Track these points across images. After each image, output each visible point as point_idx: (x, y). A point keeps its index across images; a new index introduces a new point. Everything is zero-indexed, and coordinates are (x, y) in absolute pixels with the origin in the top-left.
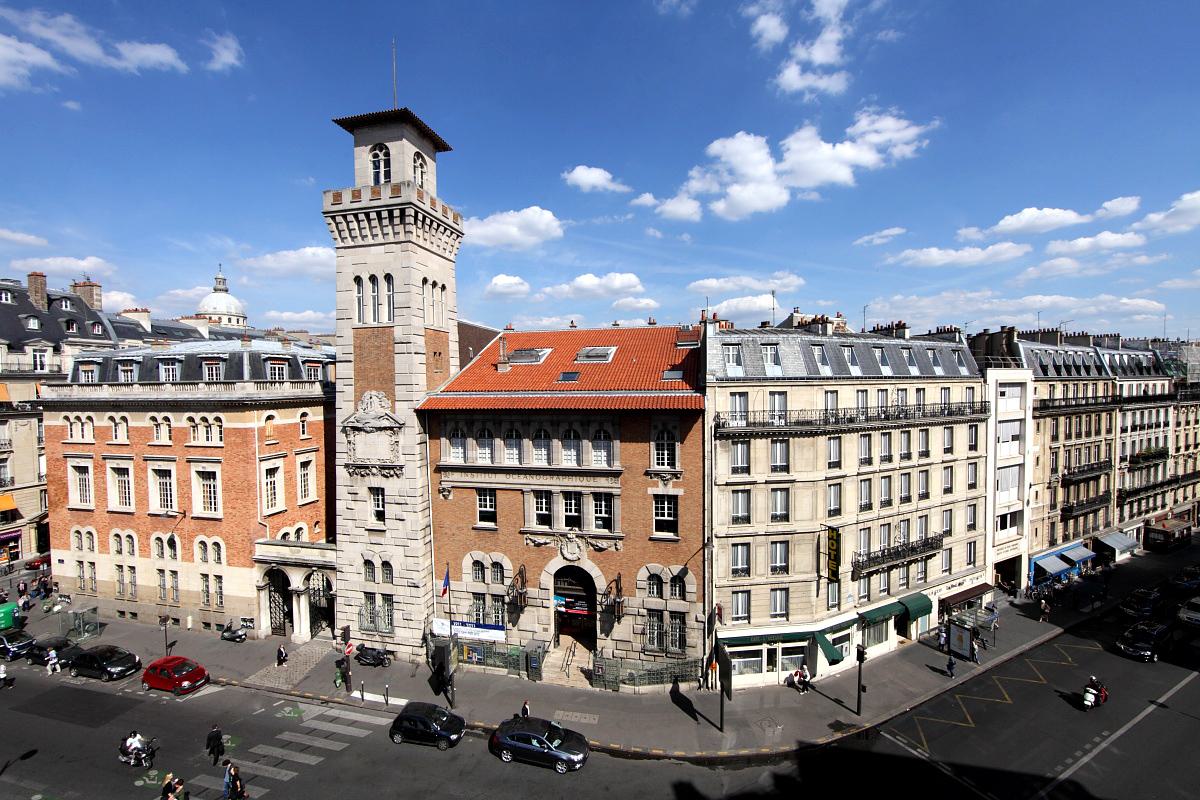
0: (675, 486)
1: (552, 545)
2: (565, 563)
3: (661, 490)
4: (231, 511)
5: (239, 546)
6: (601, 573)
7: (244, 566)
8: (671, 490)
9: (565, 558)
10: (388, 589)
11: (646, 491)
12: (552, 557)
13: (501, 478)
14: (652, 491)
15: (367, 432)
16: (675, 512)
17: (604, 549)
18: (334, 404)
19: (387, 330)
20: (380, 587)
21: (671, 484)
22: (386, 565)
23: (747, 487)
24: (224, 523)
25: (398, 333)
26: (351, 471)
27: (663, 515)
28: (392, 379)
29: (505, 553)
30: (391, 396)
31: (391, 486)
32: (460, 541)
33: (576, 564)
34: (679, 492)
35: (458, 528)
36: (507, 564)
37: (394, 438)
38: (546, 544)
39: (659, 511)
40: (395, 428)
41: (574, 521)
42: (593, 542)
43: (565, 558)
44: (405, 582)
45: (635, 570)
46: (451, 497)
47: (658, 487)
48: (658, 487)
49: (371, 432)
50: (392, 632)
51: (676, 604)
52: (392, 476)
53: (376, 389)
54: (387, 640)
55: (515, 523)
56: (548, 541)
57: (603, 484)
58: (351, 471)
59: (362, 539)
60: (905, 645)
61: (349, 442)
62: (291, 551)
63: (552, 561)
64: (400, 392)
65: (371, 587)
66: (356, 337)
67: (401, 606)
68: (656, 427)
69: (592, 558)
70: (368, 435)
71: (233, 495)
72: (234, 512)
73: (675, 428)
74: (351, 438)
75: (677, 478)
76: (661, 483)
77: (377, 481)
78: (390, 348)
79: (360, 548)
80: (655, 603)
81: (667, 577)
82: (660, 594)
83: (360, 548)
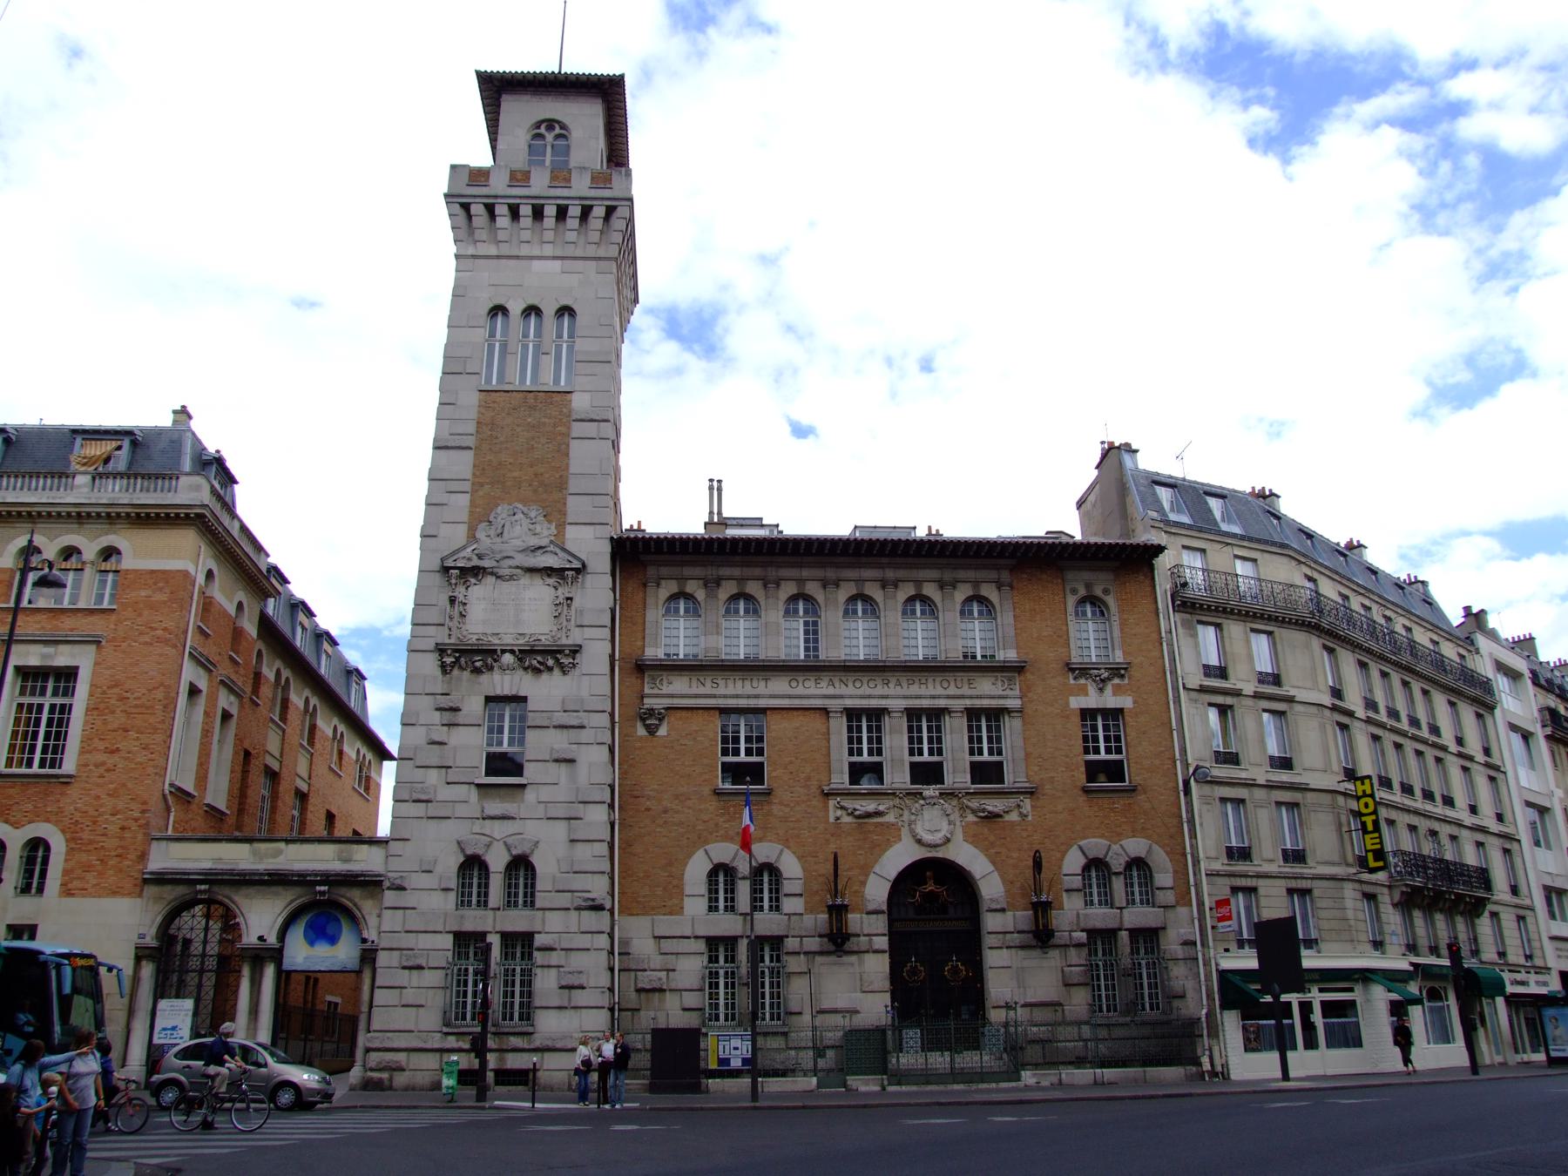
0: (1117, 691)
1: (890, 818)
2: (919, 853)
3: (1092, 700)
4: (101, 757)
5: (111, 843)
6: (992, 868)
7: (114, 893)
8: (1110, 700)
9: (919, 842)
10: (517, 920)
11: (1067, 704)
12: (888, 844)
13: (779, 685)
14: (1076, 703)
15: (498, 577)
16: (1114, 743)
17: (999, 816)
18: (518, 213)
19: (557, 398)
20: (493, 921)
21: (1109, 689)
22: (521, 865)
23: (1229, 700)
24: (73, 791)
25: (580, 402)
26: (449, 660)
27: (1097, 751)
28: (562, 485)
29: (786, 843)
30: (556, 514)
31: (545, 691)
32: (681, 823)
33: (940, 854)
34: (1126, 702)
35: (677, 797)
36: (791, 866)
37: (563, 592)
38: (878, 814)
39: (1089, 743)
40: (566, 574)
41: (927, 774)
42: (974, 804)
43: (919, 842)
44: (564, 900)
45: (1058, 855)
46: (662, 731)
47: (1087, 695)
48: (1087, 695)
49: (511, 578)
50: (527, 1016)
51: (1140, 916)
52: (550, 669)
53: (524, 502)
54: (515, 1041)
55: (808, 778)
56: (881, 808)
57: (987, 691)
58: (449, 660)
59: (461, 810)
60: (1442, 985)
61: (452, 600)
62: (255, 853)
63: (888, 853)
64: (576, 507)
65: (474, 920)
66: (484, 406)
67: (554, 958)
68: (1074, 591)
69: (973, 839)
70: (505, 585)
71: (118, 719)
72: (111, 760)
73: (1106, 592)
74: (460, 592)
75: (1122, 676)
76: (1092, 689)
77: (501, 682)
78: (561, 429)
79: (453, 831)
80: (1100, 916)
81: (1117, 864)
82: (1107, 900)
83: (453, 831)
